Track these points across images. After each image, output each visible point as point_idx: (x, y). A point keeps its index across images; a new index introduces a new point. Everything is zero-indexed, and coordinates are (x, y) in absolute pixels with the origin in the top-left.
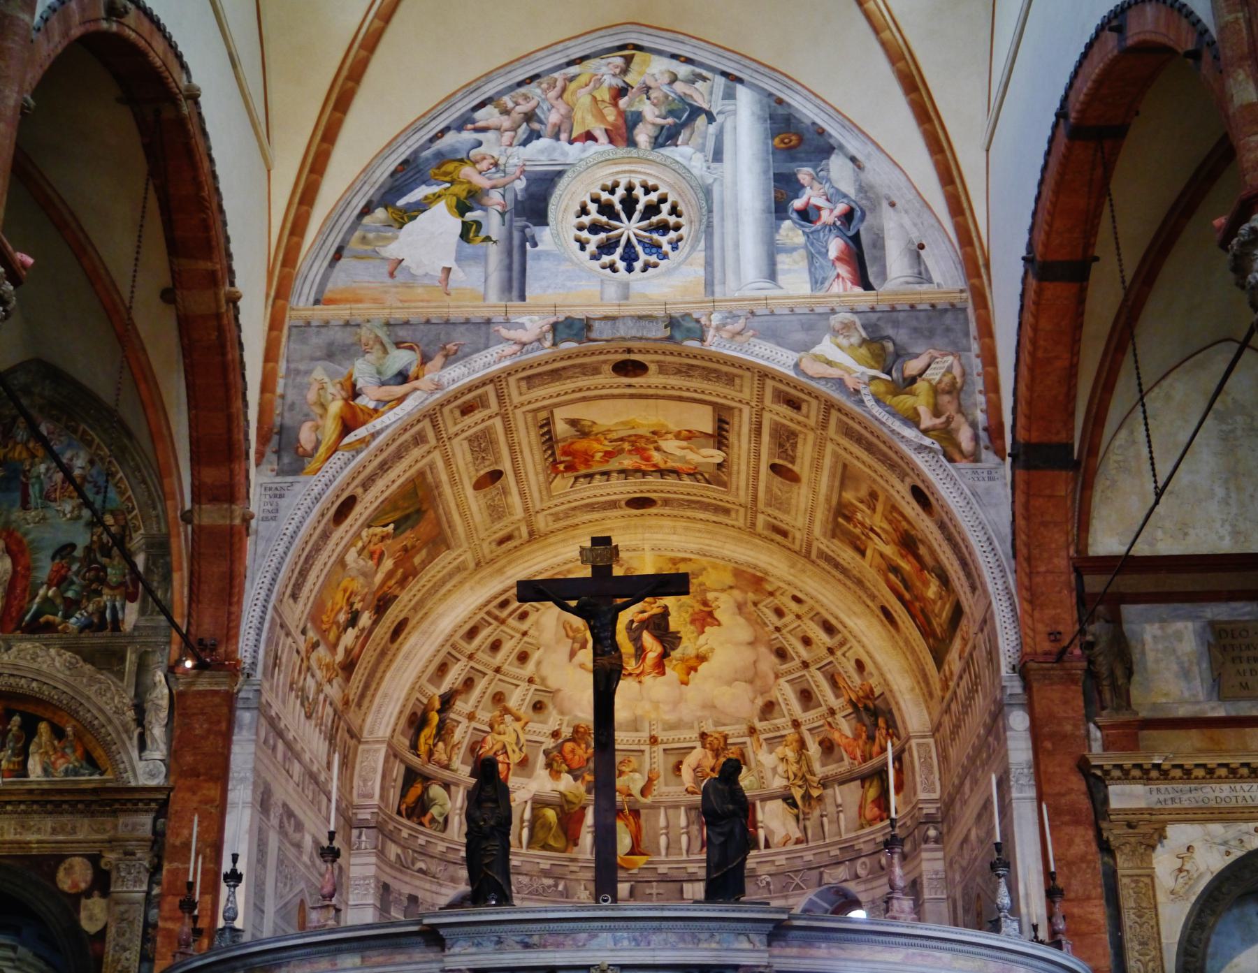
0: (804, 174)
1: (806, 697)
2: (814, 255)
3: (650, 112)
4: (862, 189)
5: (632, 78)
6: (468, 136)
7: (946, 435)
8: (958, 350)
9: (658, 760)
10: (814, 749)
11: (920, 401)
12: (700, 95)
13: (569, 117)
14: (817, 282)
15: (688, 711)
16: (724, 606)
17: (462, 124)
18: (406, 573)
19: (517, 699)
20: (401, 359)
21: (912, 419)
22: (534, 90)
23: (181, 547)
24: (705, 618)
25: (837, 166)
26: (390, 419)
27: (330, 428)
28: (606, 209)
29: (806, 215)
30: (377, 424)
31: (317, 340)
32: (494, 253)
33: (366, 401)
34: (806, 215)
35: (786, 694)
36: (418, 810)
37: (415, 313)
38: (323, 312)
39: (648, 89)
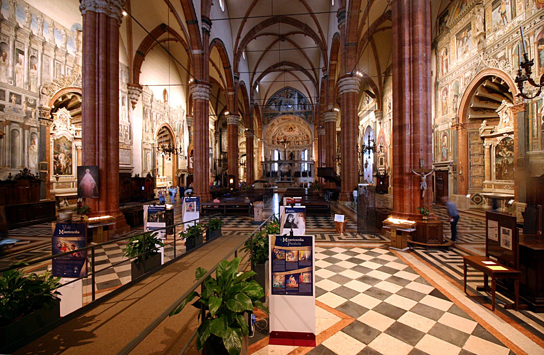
0: (301, 100)
1: (303, 134)
2: (301, 107)
4: (305, 101)
9: (291, 138)
11: (308, 119)
12: (293, 93)
14: (301, 109)
16: (296, 127)
17: (275, 96)
18: (272, 128)
19: (280, 134)
20: (271, 116)
23: (257, 131)
24: (295, 128)
25: (303, 99)
29: (301, 104)
34: (301, 104)
35: (301, 134)
36: (273, 143)
37: (273, 112)
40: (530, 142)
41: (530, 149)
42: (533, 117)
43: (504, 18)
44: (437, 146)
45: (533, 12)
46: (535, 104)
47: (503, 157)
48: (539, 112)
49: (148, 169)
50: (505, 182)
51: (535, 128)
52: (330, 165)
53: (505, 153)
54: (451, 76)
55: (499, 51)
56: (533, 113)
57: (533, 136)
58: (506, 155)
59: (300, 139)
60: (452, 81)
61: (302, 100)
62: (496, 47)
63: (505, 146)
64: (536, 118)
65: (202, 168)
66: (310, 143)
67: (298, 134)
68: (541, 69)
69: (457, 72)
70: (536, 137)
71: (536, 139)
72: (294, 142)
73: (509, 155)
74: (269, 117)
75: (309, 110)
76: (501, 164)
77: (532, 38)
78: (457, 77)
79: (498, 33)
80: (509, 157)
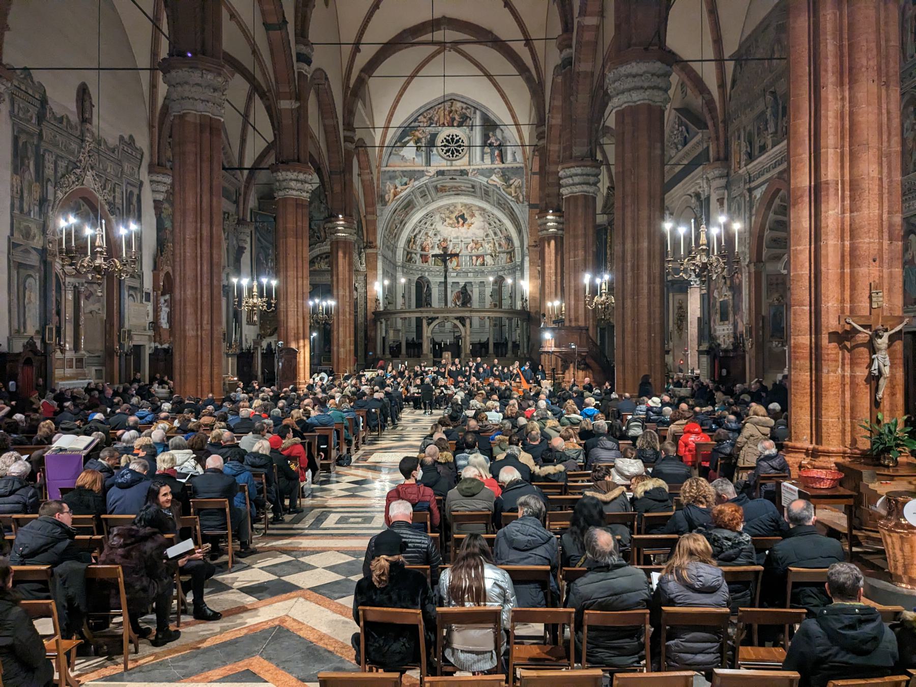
1: (495, 234)
2: (492, 154)
3: (457, 117)
4: (503, 138)
5: (453, 108)
6: (417, 124)
7: (517, 198)
8: (521, 178)
10: (497, 245)
11: (512, 190)
12: (468, 112)
13: (439, 119)
14: (492, 162)
15: (469, 235)
21: (510, 194)
22: (431, 111)
25: (498, 132)
26: (403, 194)
27: (392, 196)
28: (447, 141)
29: (491, 145)
30: (401, 195)
31: (387, 175)
32: (423, 154)
33: (399, 190)
34: (491, 145)
35: (491, 232)
38: (387, 169)
39: (456, 111)
49: (28, 327)
52: (577, 319)
59: (488, 247)
61: (494, 135)
65: (199, 325)
66: (518, 260)
67: (480, 234)
72: (471, 257)
74: (397, 182)
75: (515, 165)
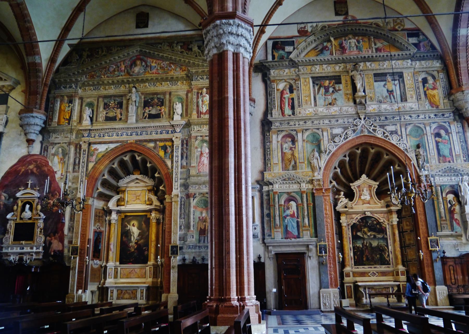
40: (439, 223)
41: (439, 230)
42: (438, 199)
43: (391, 96)
44: (269, 215)
45: (427, 107)
46: (439, 188)
47: (363, 239)
48: (444, 195)
50: (369, 268)
51: (442, 211)
53: (366, 234)
54: (301, 123)
55: (387, 123)
56: (437, 195)
57: (441, 217)
58: (368, 236)
60: (306, 130)
62: (383, 118)
63: (365, 227)
64: (441, 200)
68: (441, 158)
69: (316, 122)
70: (444, 219)
71: (444, 220)
73: (372, 236)
76: (361, 246)
77: (428, 128)
78: (317, 127)
79: (384, 106)
80: (372, 239)
